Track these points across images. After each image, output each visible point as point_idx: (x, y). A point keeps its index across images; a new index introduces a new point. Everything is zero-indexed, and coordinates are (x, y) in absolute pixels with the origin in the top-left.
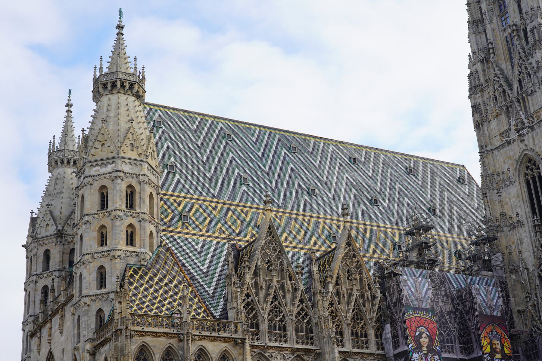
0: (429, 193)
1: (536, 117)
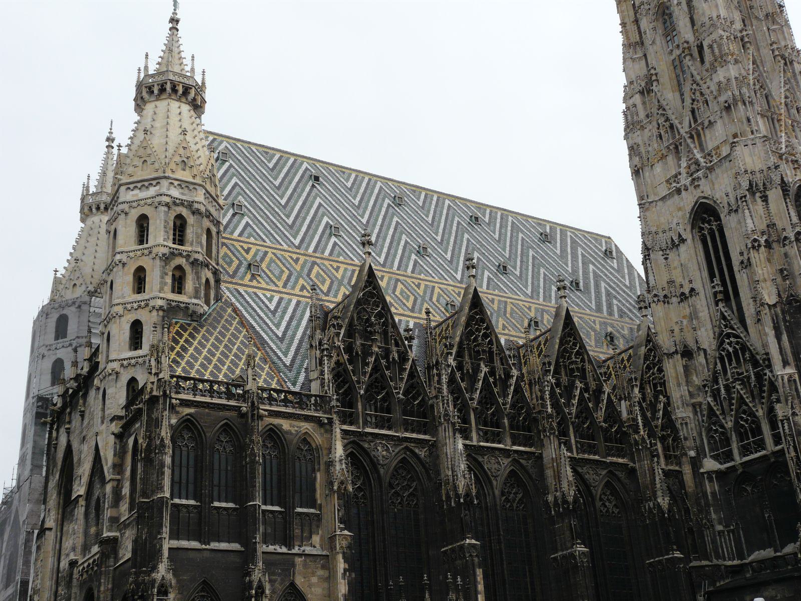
0: (570, 265)
1: (716, 154)
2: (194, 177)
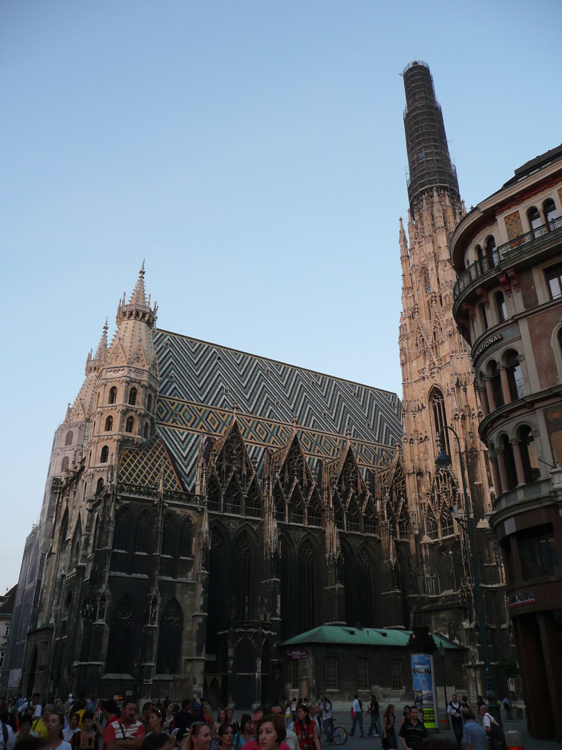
2: (144, 366)
